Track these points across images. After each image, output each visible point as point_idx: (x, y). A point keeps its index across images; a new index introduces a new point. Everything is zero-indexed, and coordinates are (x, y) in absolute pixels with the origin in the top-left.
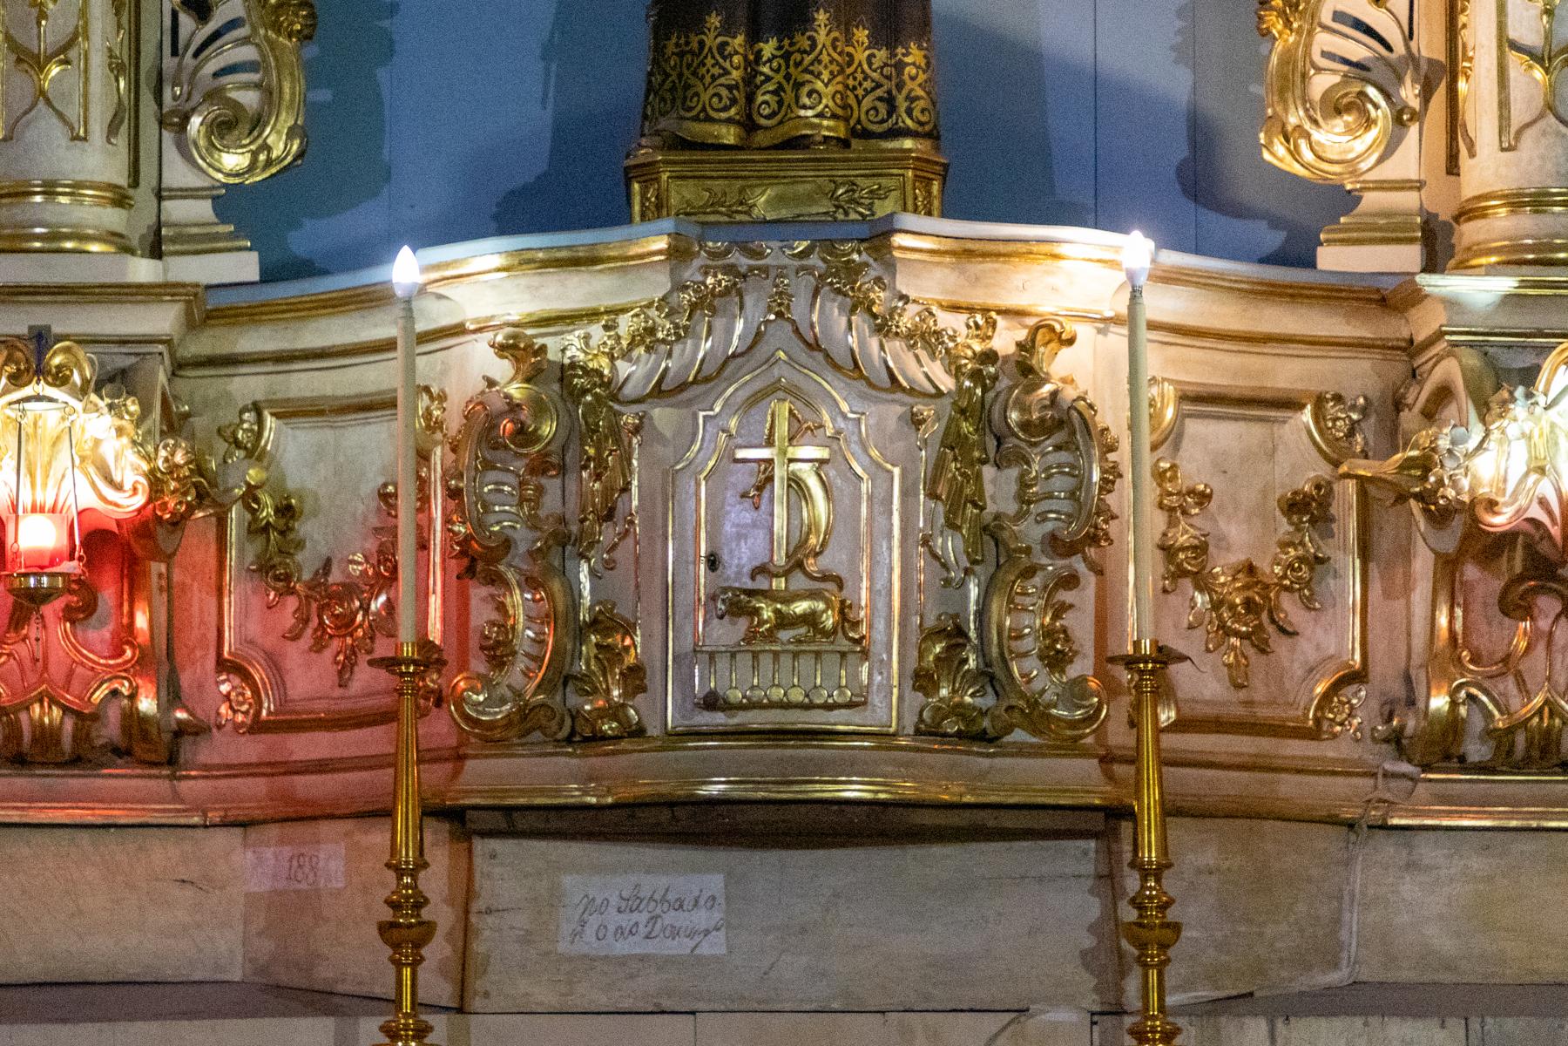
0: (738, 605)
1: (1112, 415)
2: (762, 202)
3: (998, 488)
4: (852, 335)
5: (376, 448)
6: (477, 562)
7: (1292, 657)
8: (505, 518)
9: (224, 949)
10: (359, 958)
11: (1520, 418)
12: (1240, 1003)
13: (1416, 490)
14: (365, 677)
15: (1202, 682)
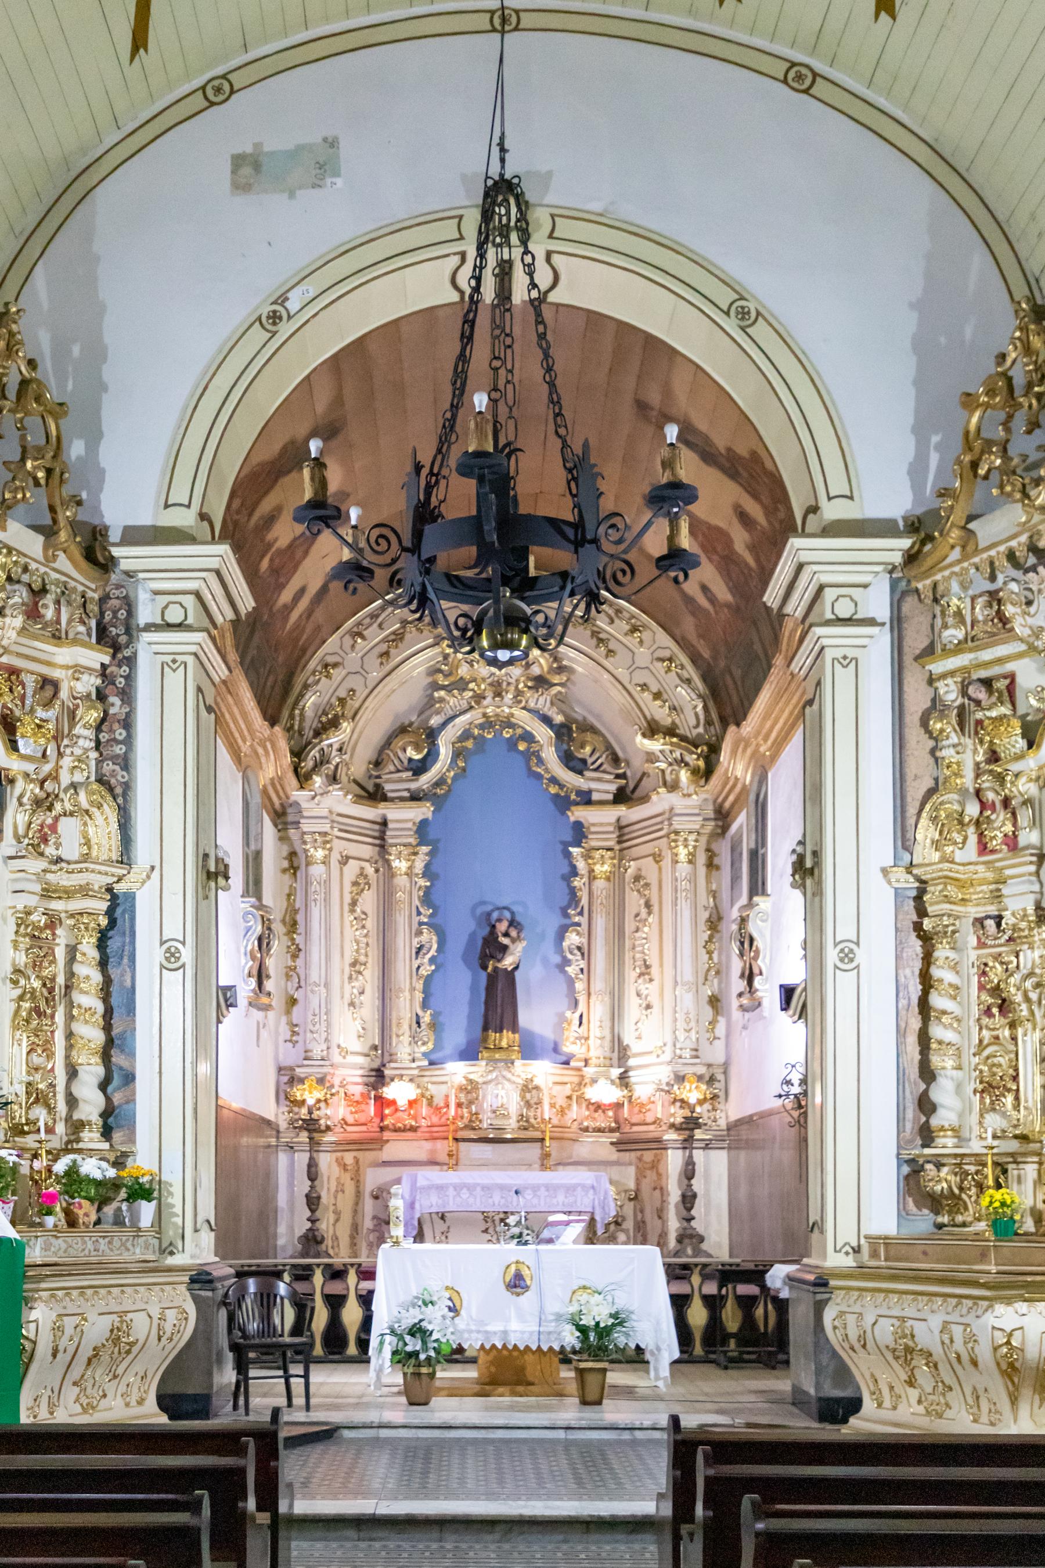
0: (494, 1112)
1: (542, 1086)
2: (497, 1056)
3: (528, 1096)
4: (509, 1076)
5: (443, 1089)
6: (459, 1105)
7: (567, 1117)
8: (463, 1100)
9: (423, 1156)
10: (443, 1157)
11: (595, 1086)
12: (559, 1164)
13: (581, 1098)
14: (443, 1120)
15: (555, 1121)
